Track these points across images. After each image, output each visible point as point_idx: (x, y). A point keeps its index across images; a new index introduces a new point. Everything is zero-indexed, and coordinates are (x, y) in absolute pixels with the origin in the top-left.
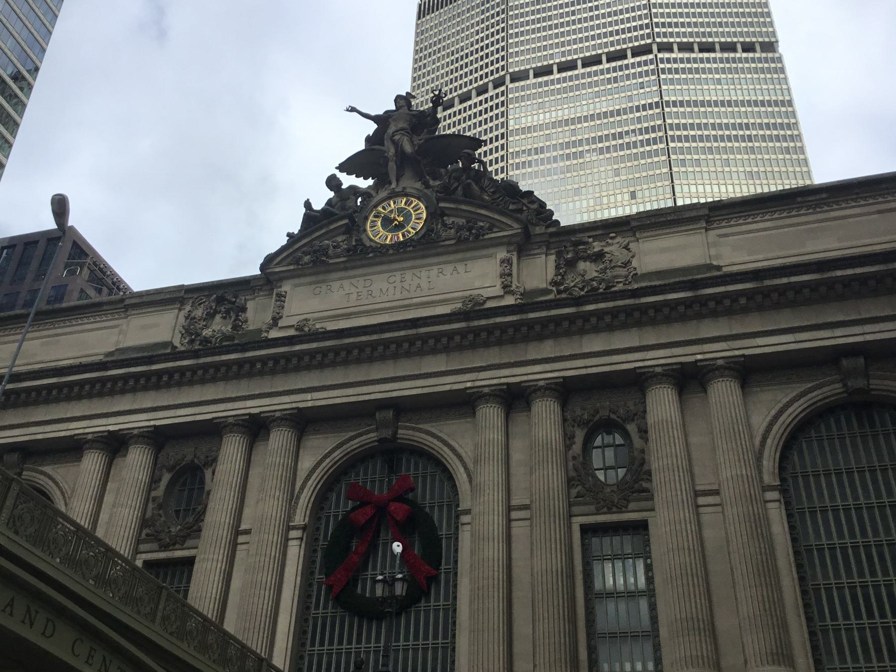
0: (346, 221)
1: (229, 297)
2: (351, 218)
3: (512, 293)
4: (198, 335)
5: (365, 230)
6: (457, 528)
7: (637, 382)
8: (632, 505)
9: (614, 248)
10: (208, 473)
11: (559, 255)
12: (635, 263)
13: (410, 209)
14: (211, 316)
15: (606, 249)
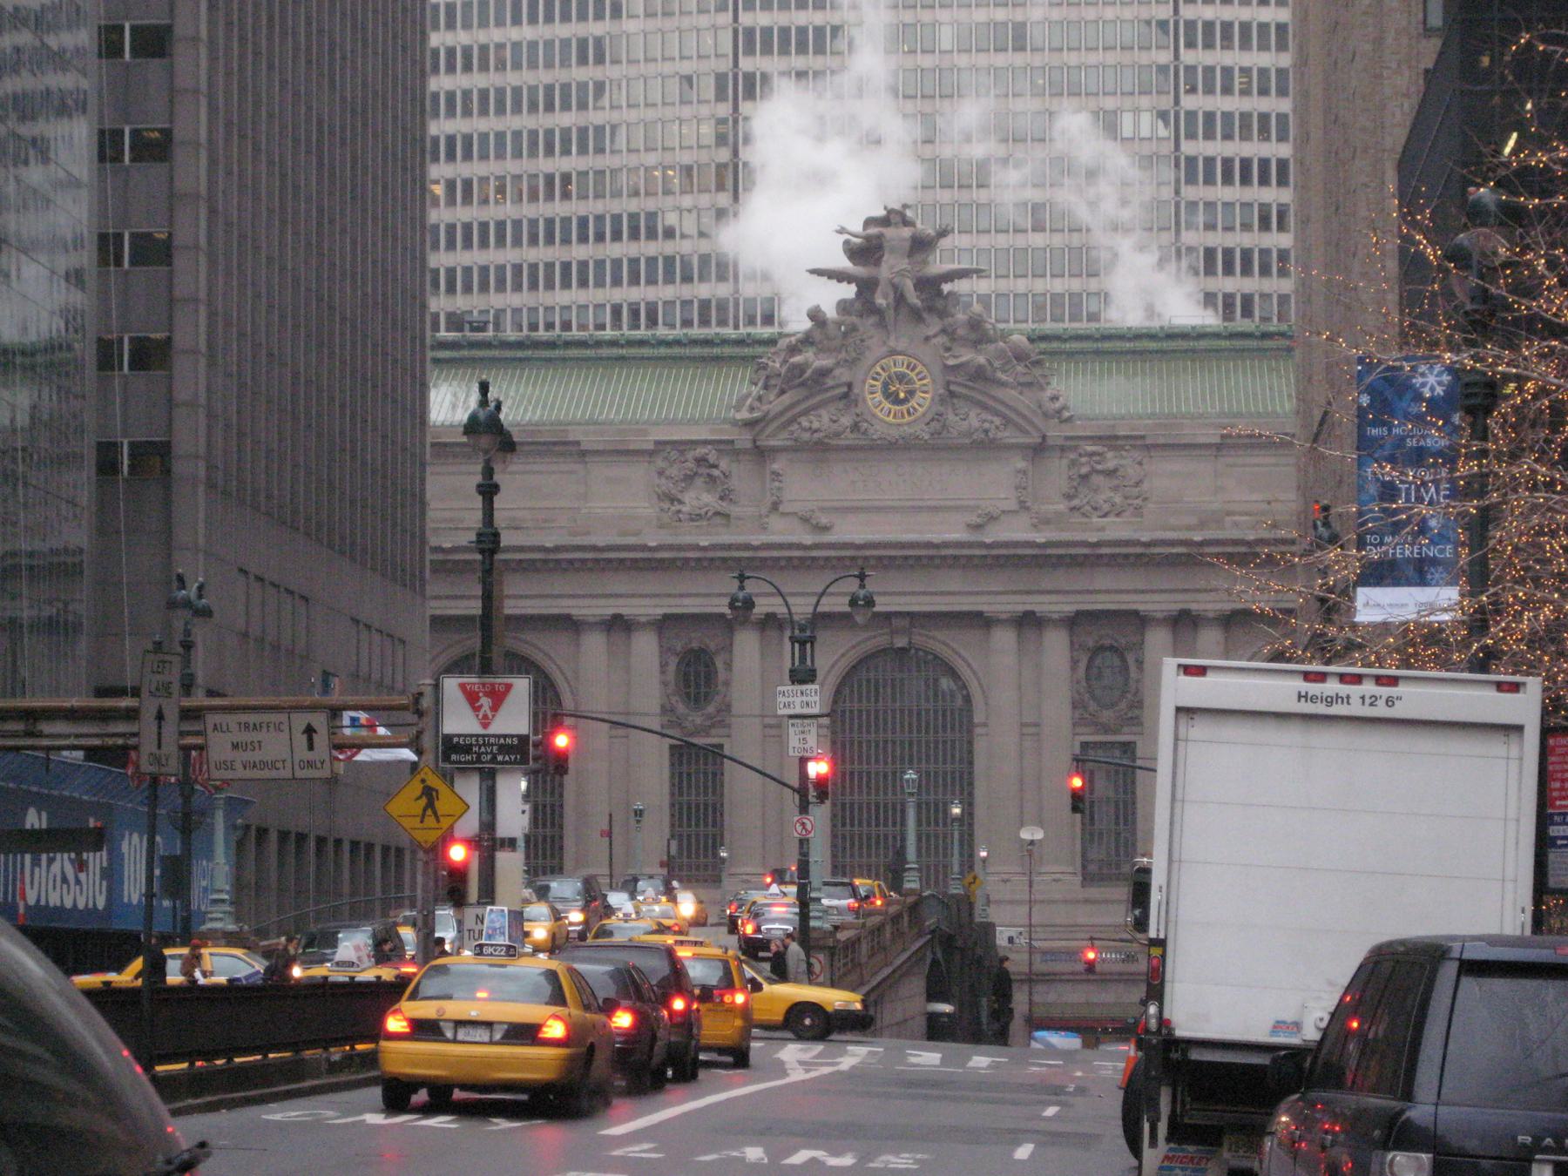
0: (845, 389)
1: (712, 458)
2: (850, 385)
3: (1028, 509)
4: (680, 502)
5: (864, 400)
6: (970, 732)
7: (1139, 621)
8: (1126, 729)
9: (1126, 462)
10: (719, 664)
11: (1073, 463)
12: (1145, 486)
13: (913, 375)
14: (689, 478)
15: (1123, 462)
